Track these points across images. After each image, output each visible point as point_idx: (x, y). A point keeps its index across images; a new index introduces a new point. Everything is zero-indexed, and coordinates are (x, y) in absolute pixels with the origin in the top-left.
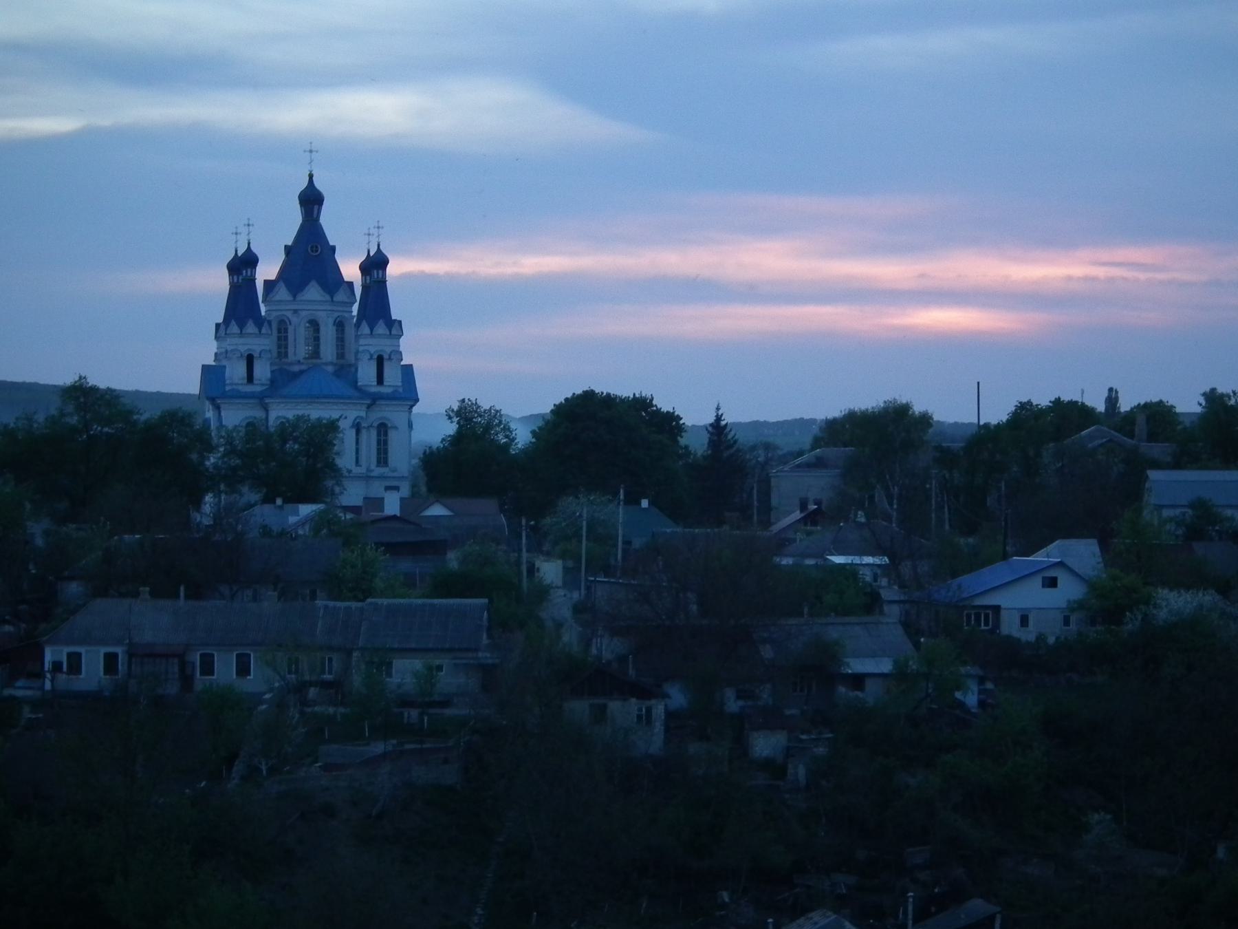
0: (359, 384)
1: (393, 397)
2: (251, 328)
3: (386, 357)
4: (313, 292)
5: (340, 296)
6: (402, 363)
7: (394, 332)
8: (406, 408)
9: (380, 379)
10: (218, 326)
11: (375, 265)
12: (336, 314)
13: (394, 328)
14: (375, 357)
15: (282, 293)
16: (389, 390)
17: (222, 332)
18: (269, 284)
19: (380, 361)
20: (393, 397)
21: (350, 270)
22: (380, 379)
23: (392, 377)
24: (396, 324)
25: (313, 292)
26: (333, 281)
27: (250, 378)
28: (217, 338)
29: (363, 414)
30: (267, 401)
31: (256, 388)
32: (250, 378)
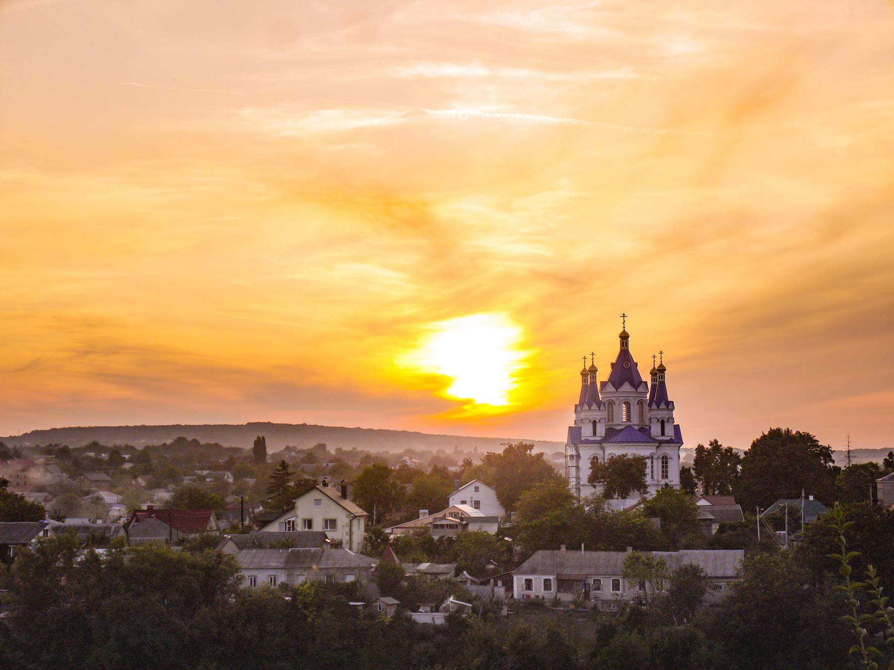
0: (652, 435)
1: (670, 442)
2: (594, 407)
3: (666, 420)
4: (627, 387)
5: (641, 389)
6: (674, 424)
7: (670, 407)
8: (677, 448)
9: (663, 434)
10: (576, 406)
11: (659, 372)
12: (639, 399)
13: (670, 405)
14: (660, 420)
15: (610, 388)
16: (668, 438)
17: (579, 409)
18: (603, 384)
19: (663, 423)
20: (670, 442)
21: (646, 377)
22: (663, 434)
23: (670, 432)
24: (671, 403)
25: (627, 387)
26: (637, 382)
27: (595, 433)
28: (575, 412)
29: (654, 451)
30: (604, 445)
31: (599, 439)
32: (595, 433)
